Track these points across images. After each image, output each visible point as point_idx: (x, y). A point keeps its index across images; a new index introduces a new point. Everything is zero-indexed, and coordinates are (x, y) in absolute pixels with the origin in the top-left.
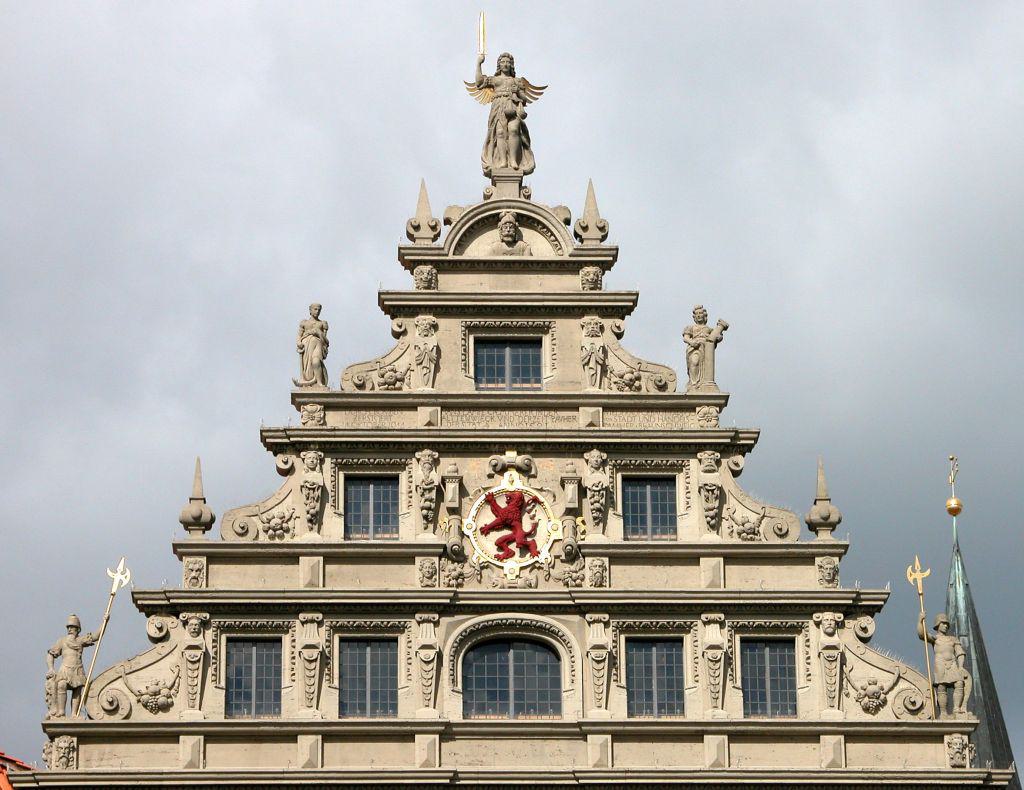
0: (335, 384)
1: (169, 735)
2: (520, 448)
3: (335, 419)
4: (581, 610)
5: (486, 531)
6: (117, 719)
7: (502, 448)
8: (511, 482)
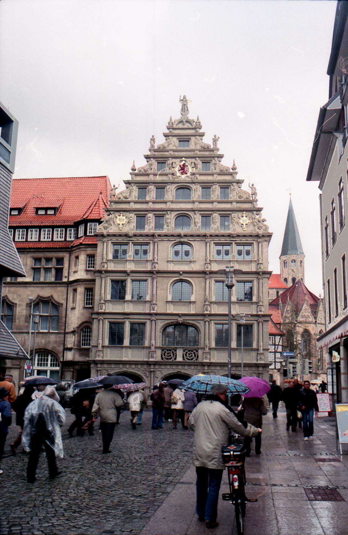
0: (156, 148)
1: (129, 202)
2: (185, 158)
3: (156, 153)
4: (194, 183)
5: (179, 171)
6: (120, 200)
7: (182, 158)
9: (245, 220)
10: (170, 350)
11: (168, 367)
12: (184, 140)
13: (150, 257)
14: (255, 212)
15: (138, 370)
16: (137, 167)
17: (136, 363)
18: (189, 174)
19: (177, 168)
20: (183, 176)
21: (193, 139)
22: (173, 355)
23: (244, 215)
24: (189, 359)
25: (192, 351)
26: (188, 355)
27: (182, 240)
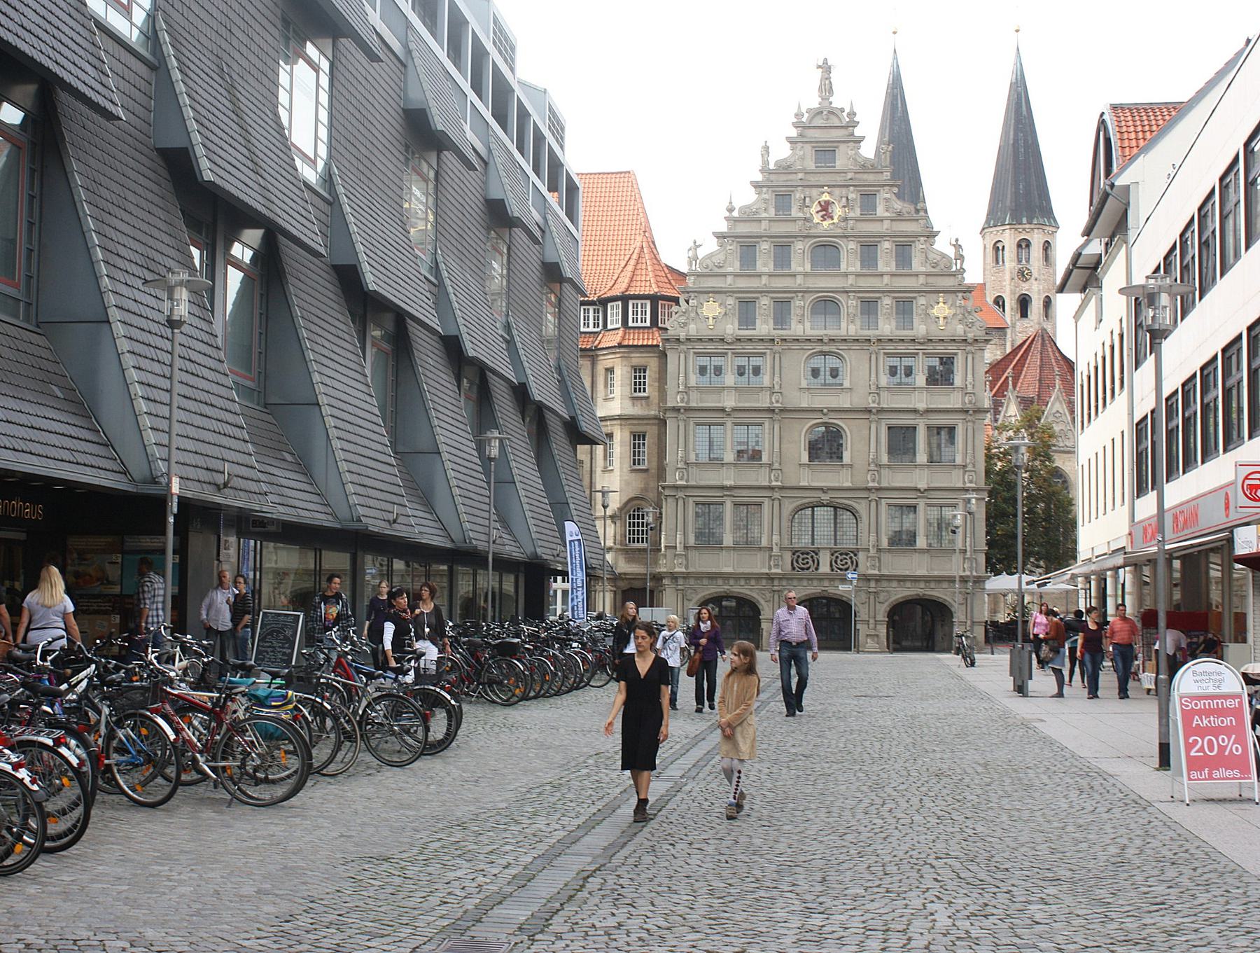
5: (817, 212)
7: (822, 186)
8: (826, 197)
9: (941, 310)
10: (808, 554)
11: (805, 583)
12: (825, 152)
13: (766, 380)
14: (960, 295)
15: (751, 590)
16: (737, 205)
17: (748, 577)
18: (836, 220)
19: (815, 208)
20: (826, 224)
21: (842, 147)
22: (813, 561)
23: (941, 300)
24: (841, 569)
25: (847, 554)
26: (839, 562)
27: (826, 348)
